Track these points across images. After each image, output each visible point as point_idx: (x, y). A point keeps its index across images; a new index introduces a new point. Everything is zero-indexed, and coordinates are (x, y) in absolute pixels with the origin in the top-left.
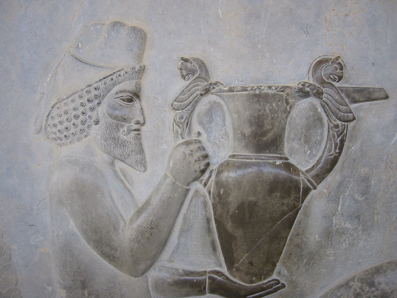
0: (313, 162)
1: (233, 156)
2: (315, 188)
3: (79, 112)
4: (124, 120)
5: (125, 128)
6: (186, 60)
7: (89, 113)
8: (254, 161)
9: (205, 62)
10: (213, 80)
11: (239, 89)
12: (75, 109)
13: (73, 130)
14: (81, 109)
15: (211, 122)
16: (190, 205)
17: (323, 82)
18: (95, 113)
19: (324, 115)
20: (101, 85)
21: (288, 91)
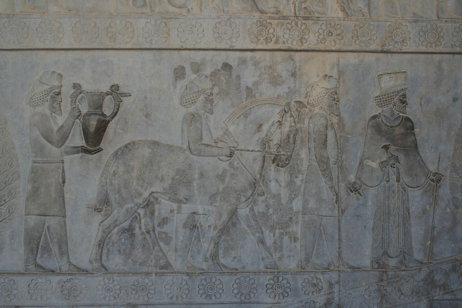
0: (110, 113)
1: (88, 112)
2: (111, 121)
3: (41, 98)
4: (56, 101)
5: (56, 103)
6: (75, 84)
7: (45, 98)
8: (93, 112)
9: (80, 84)
10: (82, 90)
11: (89, 92)
12: (40, 97)
13: (39, 103)
14: (43, 97)
15: (82, 102)
16: (75, 126)
17: (113, 91)
18: (47, 98)
19: (113, 100)
20: (49, 90)
21: (103, 93)
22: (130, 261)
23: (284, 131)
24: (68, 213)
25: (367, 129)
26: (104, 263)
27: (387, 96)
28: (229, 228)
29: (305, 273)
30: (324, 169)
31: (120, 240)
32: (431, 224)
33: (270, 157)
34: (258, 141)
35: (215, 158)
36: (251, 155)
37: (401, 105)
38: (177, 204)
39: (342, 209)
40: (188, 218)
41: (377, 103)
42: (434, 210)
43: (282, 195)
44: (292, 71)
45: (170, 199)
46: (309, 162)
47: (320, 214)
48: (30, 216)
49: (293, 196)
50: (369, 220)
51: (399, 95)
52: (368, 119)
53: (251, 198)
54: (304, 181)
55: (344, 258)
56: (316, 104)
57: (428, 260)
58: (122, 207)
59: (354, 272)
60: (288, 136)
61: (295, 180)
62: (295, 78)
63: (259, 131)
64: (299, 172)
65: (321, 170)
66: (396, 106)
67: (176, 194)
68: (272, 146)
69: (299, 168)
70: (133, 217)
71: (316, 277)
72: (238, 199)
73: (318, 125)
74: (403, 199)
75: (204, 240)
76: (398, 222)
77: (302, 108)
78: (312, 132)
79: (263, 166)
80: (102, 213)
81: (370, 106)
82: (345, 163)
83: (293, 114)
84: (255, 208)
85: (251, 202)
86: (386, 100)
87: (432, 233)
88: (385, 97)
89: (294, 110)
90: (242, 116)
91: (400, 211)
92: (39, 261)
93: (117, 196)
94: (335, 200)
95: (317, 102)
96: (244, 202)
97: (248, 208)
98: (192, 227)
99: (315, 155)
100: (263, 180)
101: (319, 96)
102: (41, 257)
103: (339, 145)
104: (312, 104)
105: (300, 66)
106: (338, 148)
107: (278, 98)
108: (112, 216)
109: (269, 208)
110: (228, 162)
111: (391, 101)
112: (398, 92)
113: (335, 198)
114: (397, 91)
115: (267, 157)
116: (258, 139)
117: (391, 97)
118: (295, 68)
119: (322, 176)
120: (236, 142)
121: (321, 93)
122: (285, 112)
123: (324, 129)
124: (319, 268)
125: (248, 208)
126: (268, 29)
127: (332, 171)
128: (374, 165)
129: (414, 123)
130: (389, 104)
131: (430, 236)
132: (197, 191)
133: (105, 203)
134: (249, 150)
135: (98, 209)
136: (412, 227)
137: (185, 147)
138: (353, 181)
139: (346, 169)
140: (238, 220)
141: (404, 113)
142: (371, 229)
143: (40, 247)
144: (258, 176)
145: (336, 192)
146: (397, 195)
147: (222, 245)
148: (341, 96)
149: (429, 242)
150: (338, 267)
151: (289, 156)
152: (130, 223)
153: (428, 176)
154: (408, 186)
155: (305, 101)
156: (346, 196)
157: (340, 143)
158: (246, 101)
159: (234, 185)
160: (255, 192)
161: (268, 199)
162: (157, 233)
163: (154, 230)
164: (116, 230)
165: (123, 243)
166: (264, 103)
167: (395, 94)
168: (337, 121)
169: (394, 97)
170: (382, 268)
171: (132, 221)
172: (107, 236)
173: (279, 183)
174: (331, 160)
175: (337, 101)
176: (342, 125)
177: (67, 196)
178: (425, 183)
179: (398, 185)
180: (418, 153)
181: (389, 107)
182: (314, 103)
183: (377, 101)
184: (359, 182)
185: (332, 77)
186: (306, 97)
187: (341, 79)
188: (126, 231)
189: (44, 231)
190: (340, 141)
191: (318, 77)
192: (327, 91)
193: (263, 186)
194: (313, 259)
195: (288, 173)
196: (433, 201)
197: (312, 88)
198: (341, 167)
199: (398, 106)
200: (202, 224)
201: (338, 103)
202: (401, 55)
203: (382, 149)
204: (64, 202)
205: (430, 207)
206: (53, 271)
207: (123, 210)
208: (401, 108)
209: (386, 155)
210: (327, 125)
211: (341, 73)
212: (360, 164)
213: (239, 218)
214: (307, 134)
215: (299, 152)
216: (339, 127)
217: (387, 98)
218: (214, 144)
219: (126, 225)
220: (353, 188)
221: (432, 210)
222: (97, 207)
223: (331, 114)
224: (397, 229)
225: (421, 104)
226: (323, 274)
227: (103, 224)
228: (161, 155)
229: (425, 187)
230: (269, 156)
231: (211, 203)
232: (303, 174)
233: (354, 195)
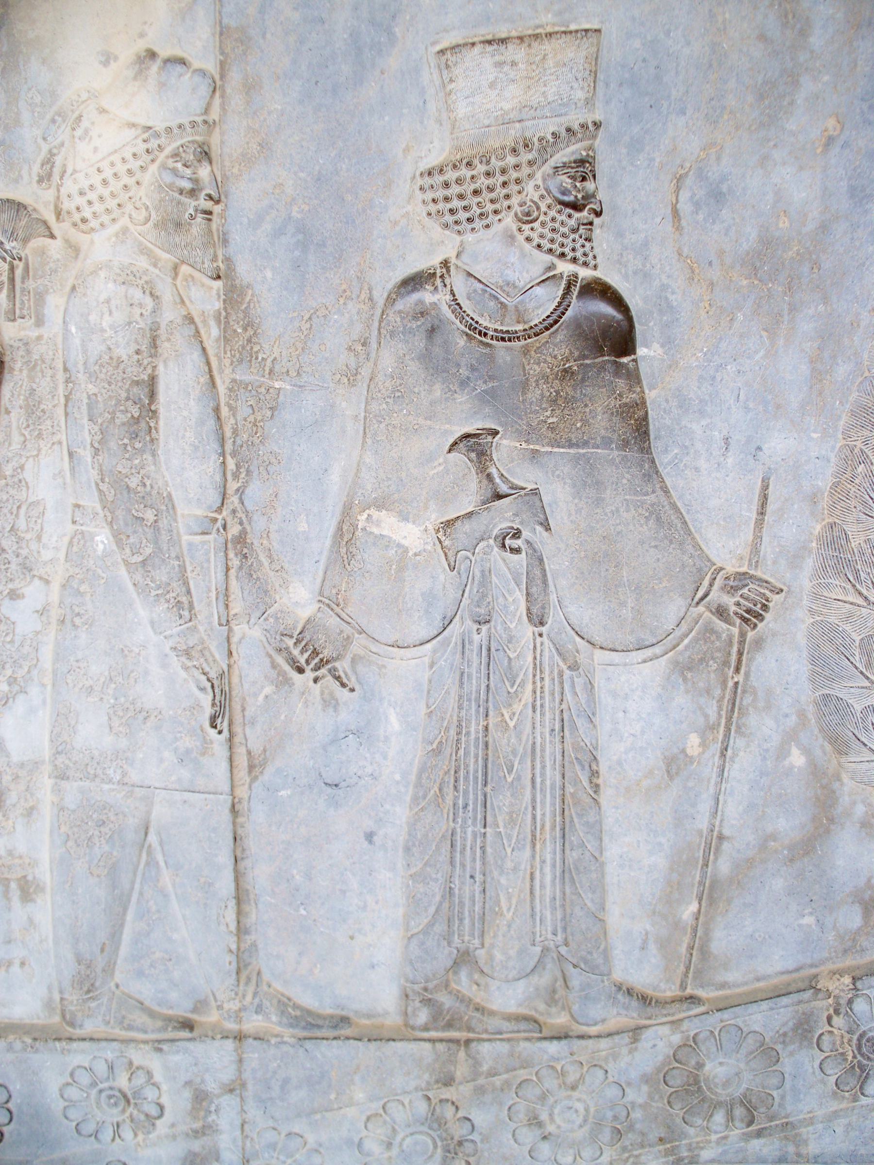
25: (374, 345)
27: (481, 168)
29: (75, 1045)
30: (141, 559)
32: (703, 824)
37: (564, 217)
39: (249, 753)
42: (723, 755)
46: (74, 522)
47: (134, 776)
50: (387, 807)
51: (552, 162)
52: (385, 295)
55: (266, 976)
57: (683, 987)
59: (308, 1045)
65: (126, 563)
66: (536, 225)
71: (131, 1063)
73: (103, 330)
74: (564, 706)
76: (534, 817)
78: (81, 368)
81: (396, 223)
82: (259, 523)
86: (476, 192)
87: (706, 865)
88: (469, 174)
91: (543, 767)
94: (208, 711)
95: (98, 207)
99: (97, 485)
101: (108, 173)
103: (228, 433)
104: (77, 217)
106: (223, 446)
111: (507, 197)
113: (206, 700)
114: (540, 140)
117: (503, 171)
119: (135, 595)
121: (116, 158)
123: (138, 352)
124: (141, 1019)
127: (189, 568)
129: (633, 313)
130: (496, 212)
131: (698, 878)
136: (606, 839)
138: (304, 613)
139: (270, 557)
141: (582, 259)
142: (401, 850)
145: (213, 675)
146: (529, 687)
148: (235, 171)
149: (694, 907)
150: (238, 1016)
153: (700, 594)
156: (268, 690)
157: (232, 421)
167: (530, 156)
168: (218, 305)
169: (526, 170)
170: (449, 1026)
174: (182, 509)
175: (210, 197)
176: (245, 329)
178: (684, 627)
179: (539, 639)
182: (87, 213)
183: (429, 195)
184: (333, 621)
187: (235, 76)
192: (153, 144)
194: (118, 977)
196: (720, 716)
197: (74, 129)
199: (543, 224)
201: (217, 209)
203: (453, 454)
205: (704, 744)
208: (564, 235)
212: (340, 529)
216: (226, 337)
217: (482, 182)
220: (302, 652)
221: (714, 755)
223: (185, 269)
224: (527, 853)
225: (675, 213)
226: (160, 1050)
229: (681, 647)
233: (311, 683)
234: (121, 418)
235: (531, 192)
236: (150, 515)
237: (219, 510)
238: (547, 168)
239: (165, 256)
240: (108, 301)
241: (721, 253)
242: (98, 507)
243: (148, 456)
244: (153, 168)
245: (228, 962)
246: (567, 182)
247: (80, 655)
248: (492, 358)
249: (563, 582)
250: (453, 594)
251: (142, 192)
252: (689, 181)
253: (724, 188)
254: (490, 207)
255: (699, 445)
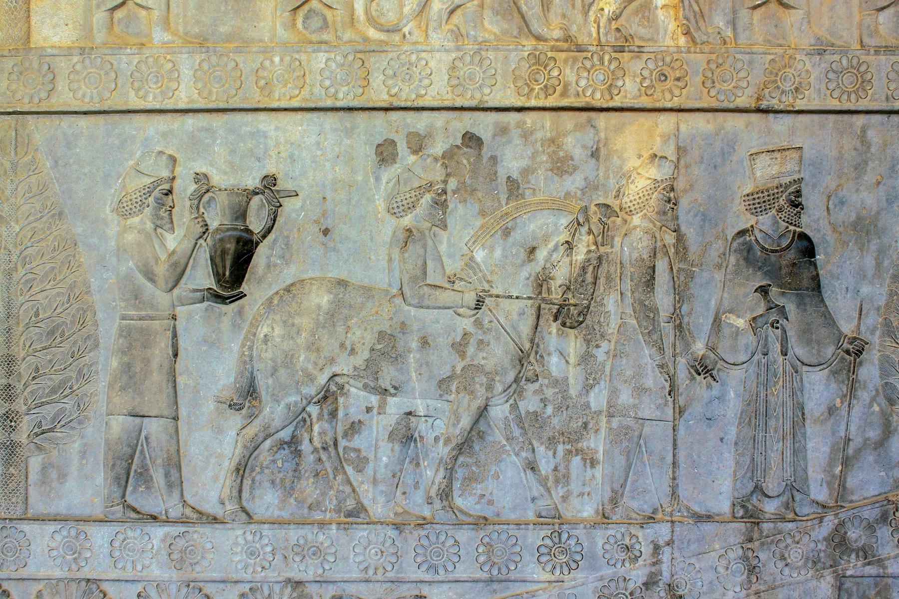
22: (292, 500)
23: (576, 261)
24: (183, 412)
25: (728, 255)
26: (245, 504)
27: (766, 194)
28: (473, 442)
31: (274, 462)
33: (549, 309)
34: (528, 279)
35: (448, 310)
36: (515, 306)
38: (378, 397)
40: (398, 423)
41: (748, 207)
43: (571, 381)
44: (592, 147)
45: (366, 387)
46: (621, 319)
48: (116, 417)
49: (591, 382)
51: (788, 192)
53: (514, 386)
54: (611, 353)
56: (635, 209)
58: (278, 402)
60: (584, 269)
61: (595, 351)
62: (598, 159)
63: (530, 261)
64: (602, 336)
67: (377, 379)
68: (553, 289)
69: (602, 330)
70: (298, 419)
72: (489, 388)
73: (638, 249)
75: (426, 463)
77: (609, 218)
78: (628, 262)
79: (537, 324)
80: (244, 411)
83: (593, 228)
84: (522, 405)
85: (515, 392)
86: (764, 202)
89: (596, 221)
90: (500, 233)
92: (130, 499)
93: (270, 381)
96: (501, 394)
97: (508, 404)
98: (404, 440)
99: (632, 304)
100: (537, 353)
101: (641, 195)
102: (134, 491)
104: (628, 210)
105: (606, 139)
107: (565, 198)
108: (261, 417)
109: (545, 405)
110: (473, 319)
111: (774, 203)
112: (787, 187)
115: (545, 309)
116: (528, 276)
117: (773, 194)
118: (598, 141)
120: (488, 281)
122: (579, 224)
123: (650, 257)
125: (508, 404)
126: (548, 68)
128: (741, 323)
130: (770, 208)
132: (416, 372)
133: (248, 395)
134: (510, 297)
135: (235, 404)
137: (394, 291)
139: (689, 332)
140: (489, 426)
143: (132, 474)
144: (527, 346)
147: (460, 473)
151: (585, 307)
152: (294, 431)
153: (840, 344)
154: (802, 363)
155: (615, 204)
158: (506, 204)
159: (483, 362)
160: (521, 375)
161: (544, 388)
162: (341, 450)
163: (336, 444)
164: (268, 443)
165: (281, 468)
166: (540, 208)
168: (674, 241)
171: (296, 427)
172: (251, 454)
173: (565, 357)
175: (674, 204)
177: (181, 380)
180: (822, 301)
181: (771, 214)
182: (632, 209)
183: (747, 203)
185: (666, 158)
186: (617, 197)
187: (682, 162)
188: (285, 446)
189: (140, 444)
190: (678, 278)
191: (639, 158)
192: (657, 185)
193: (536, 364)
195: (582, 339)
198: (679, 327)
200: (423, 434)
201: (675, 208)
202: (792, 116)
204: (176, 392)
206: (154, 518)
207: (281, 406)
209: (762, 305)
210: (655, 248)
211: (681, 151)
212: (715, 321)
213: (491, 423)
214: (619, 266)
215: (603, 299)
217: (767, 198)
218: (447, 285)
219: (285, 434)
222: (235, 401)
225: (828, 209)
227: (244, 431)
228: (351, 306)
230: (548, 306)
231: (441, 396)
232: (610, 341)
234: (644, 280)
235: (781, 202)
236: (652, 315)
237: (673, 314)
238: (787, 193)
239: (658, 223)
240: (641, 239)
241: (844, 222)
242: (632, 313)
243: (651, 294)
244: (656, 193)
245: (668, 490)
246: (793, 198)
247: (623, 368)
248: (769, 259)
249: (793, 340)
250: (755, 344)
251: (652, 202)
252: (832, 198)
253: (844, 200)
254: (768, 207)
255: (837, 290)
